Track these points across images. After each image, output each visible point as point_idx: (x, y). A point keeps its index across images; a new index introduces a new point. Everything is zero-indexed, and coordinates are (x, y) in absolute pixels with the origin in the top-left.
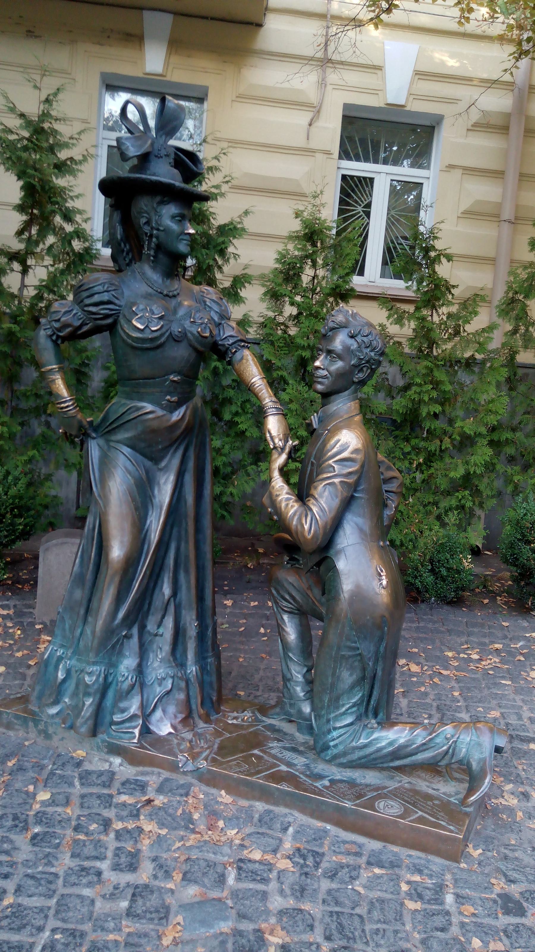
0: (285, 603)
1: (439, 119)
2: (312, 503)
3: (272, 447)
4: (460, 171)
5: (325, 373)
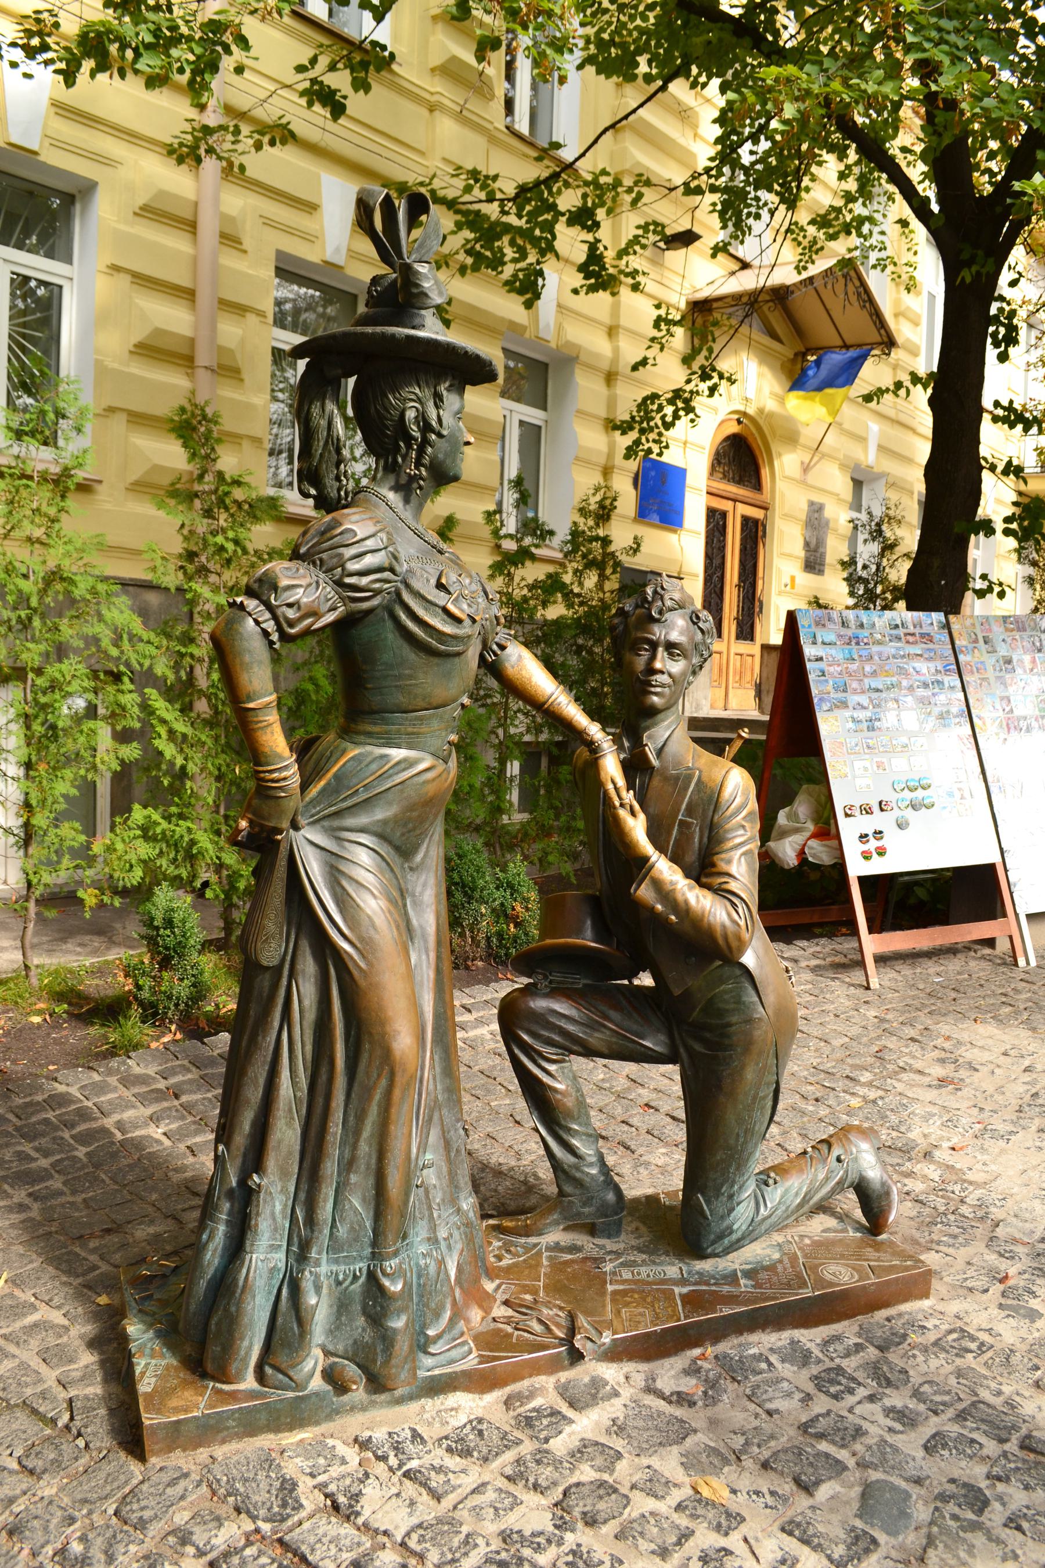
0: (546, 1050)
1: (88, 188)
2: (733, 886)
3: (617, 803)
4: (128, 278)
5: (664, 679)
